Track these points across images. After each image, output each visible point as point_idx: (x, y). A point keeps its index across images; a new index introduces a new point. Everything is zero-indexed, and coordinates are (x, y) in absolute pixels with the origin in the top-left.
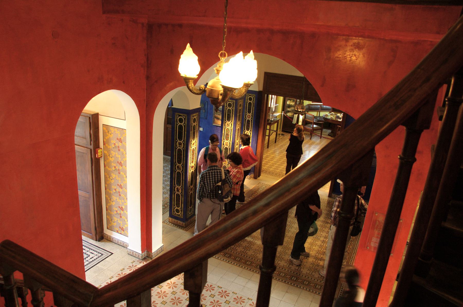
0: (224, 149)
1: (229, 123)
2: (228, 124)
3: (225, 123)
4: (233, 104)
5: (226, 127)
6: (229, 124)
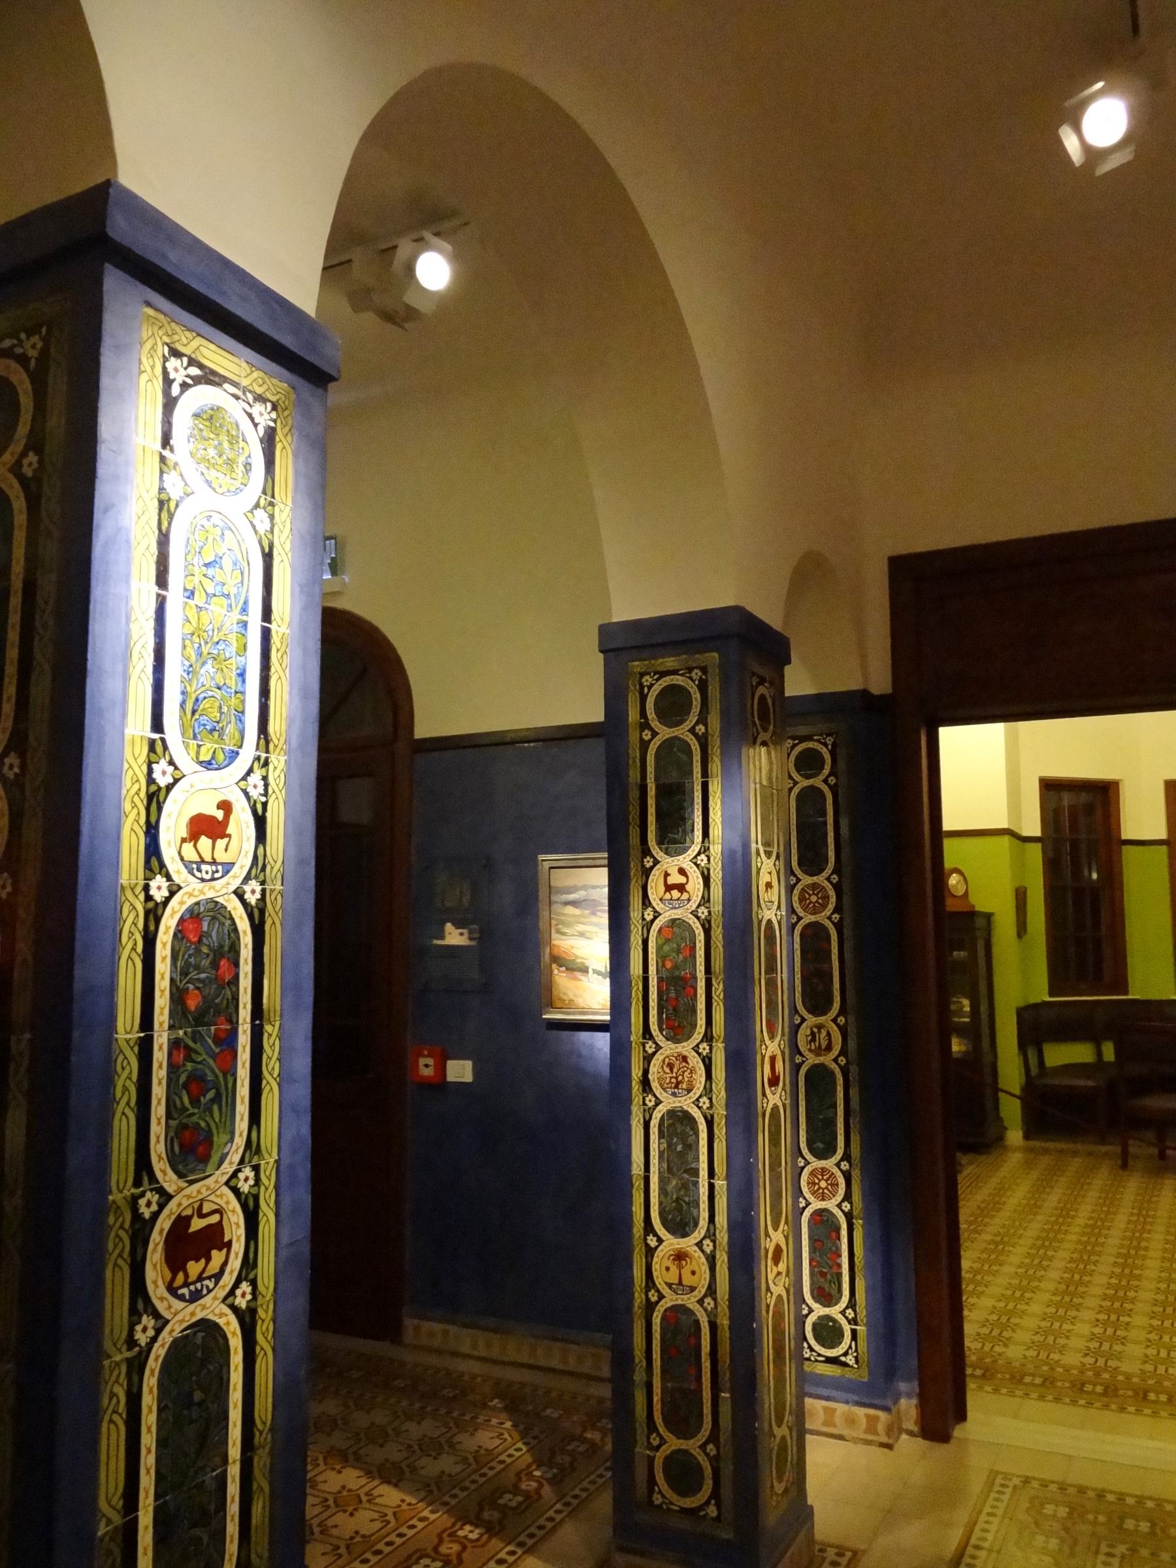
0: (661, 1135)
1: (682, 871)
2: (675, 878)
3: (647, 872)
4: (703, 686)
5: (657, 914)
6: (682, 880)
